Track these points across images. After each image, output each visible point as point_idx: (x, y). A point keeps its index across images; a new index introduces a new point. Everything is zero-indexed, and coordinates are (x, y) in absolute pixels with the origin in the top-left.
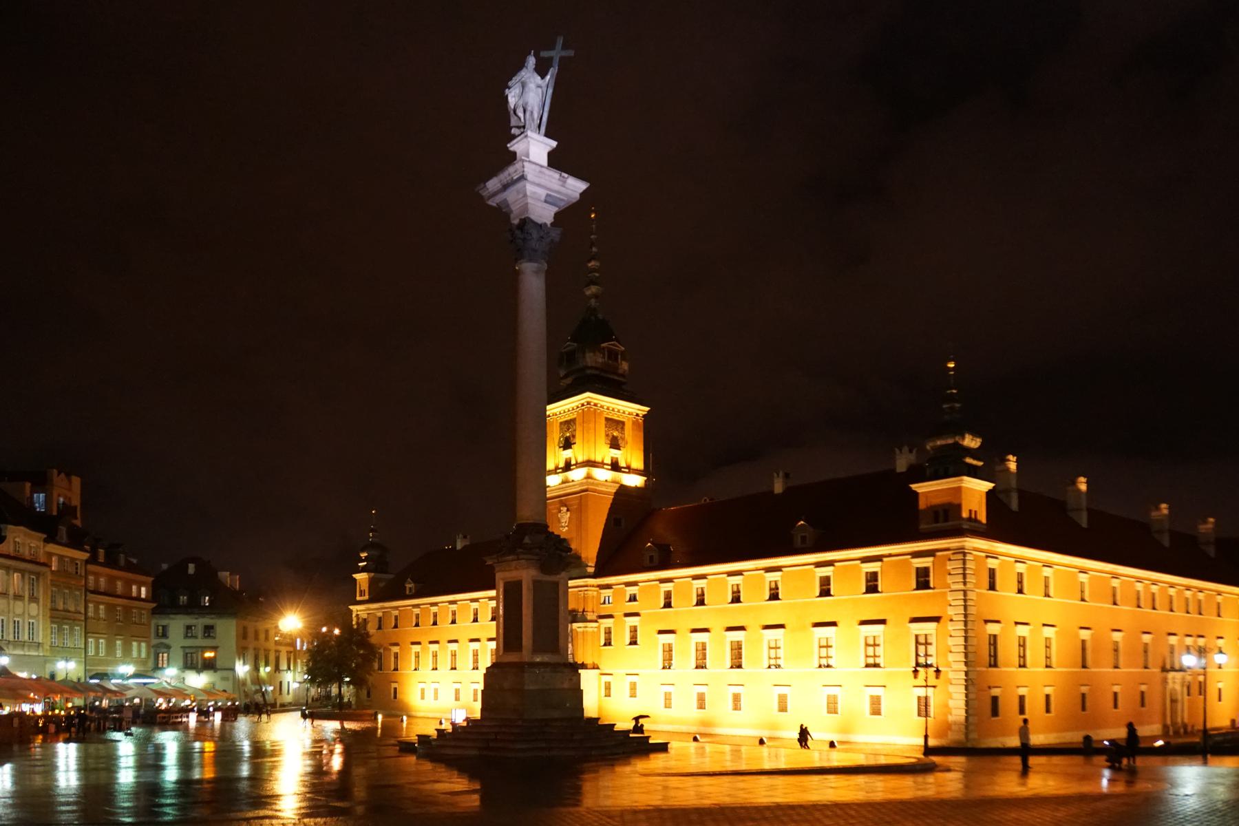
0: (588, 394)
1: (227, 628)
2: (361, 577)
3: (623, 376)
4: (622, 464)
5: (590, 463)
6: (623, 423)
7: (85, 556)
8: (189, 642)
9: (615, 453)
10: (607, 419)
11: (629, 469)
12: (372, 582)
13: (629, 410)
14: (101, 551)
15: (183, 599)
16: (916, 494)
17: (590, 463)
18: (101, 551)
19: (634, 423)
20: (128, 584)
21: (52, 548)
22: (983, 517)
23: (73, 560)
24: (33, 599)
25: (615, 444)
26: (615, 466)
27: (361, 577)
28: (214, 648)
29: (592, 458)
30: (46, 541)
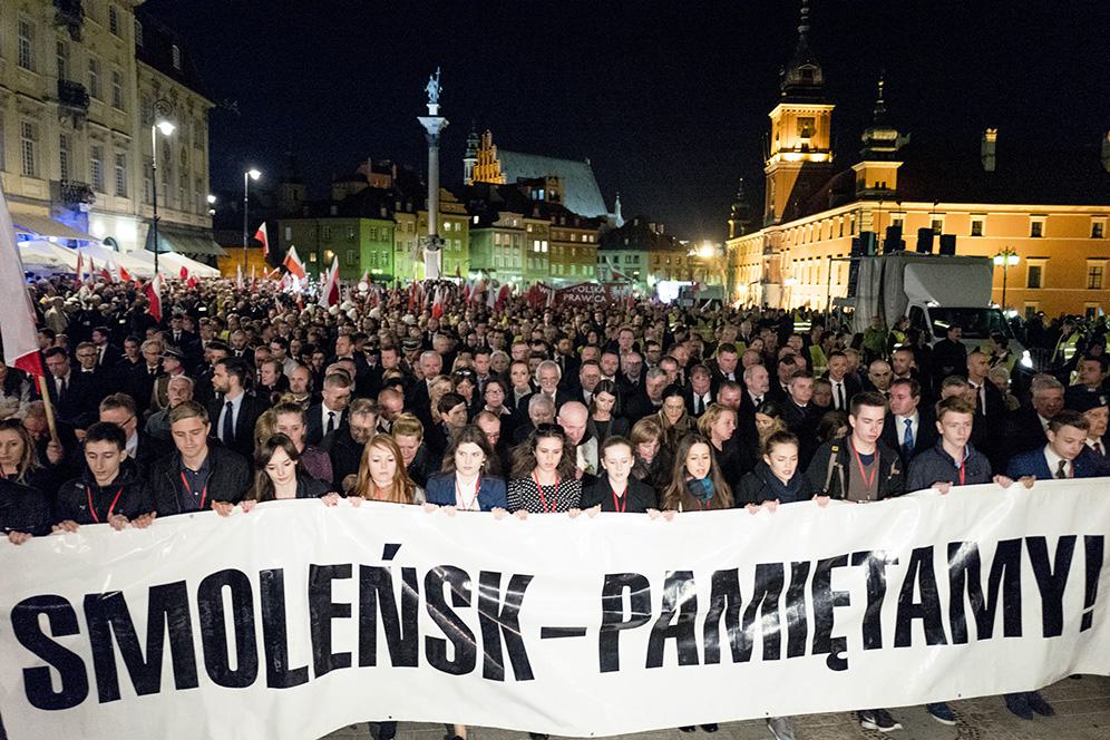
0: (781, 105)
1: (644, 256)
2: (731, 222)
3: (818, 85)
4: (811, 146)
5: (783, 150)
6: (813, 119)
7: (549, 223)
8: (629, 266)
9: (805, 140)
10: (799, 118)
11: (817, 150)
12: (735, 225)
13: (815, 110)
14: (563, 219)
15: (627, 241)
16: (855, 172)
17: (783, 150)
18: (563, 219)
19: (822, 118)
20: (580, 236)
21: (527, 220)
22: (894, 187)
23: (541, 226)
24: (515, 246)
25: (805, 134)
26: (805, 149)
27: (731, 222)
28: (638, 269)
29: (784, 146)
30: (524, 217)
